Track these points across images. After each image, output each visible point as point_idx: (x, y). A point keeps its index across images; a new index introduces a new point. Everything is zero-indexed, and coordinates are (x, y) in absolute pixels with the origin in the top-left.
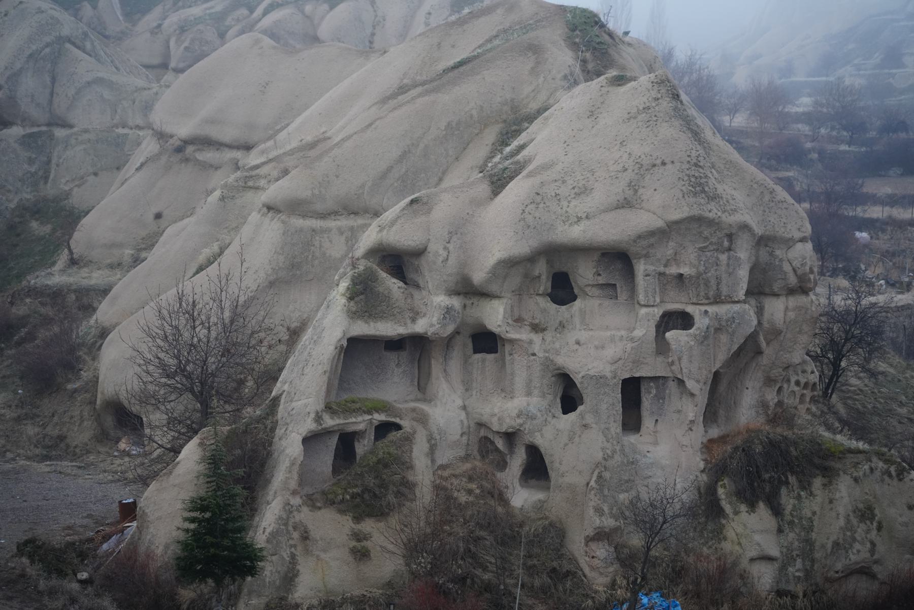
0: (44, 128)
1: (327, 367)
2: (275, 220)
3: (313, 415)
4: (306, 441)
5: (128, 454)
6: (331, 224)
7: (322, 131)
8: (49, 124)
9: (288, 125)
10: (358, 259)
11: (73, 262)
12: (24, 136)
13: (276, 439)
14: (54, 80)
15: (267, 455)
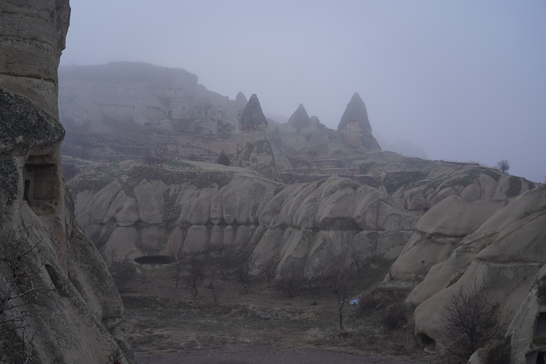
0: (374, 231)
1: (533, 325)
2: (484, 264)
3: (529, 345)
4: (527, 355)
5: (429, 354)
6: (508, 265)
7: (494, 230)
8: (376, 230)
9: (478, 228)
10: (539, 280)
11: (392, 279)
12: (368, 234)
13: (512, 354)
14: (378, 214)
15: (509, 360)
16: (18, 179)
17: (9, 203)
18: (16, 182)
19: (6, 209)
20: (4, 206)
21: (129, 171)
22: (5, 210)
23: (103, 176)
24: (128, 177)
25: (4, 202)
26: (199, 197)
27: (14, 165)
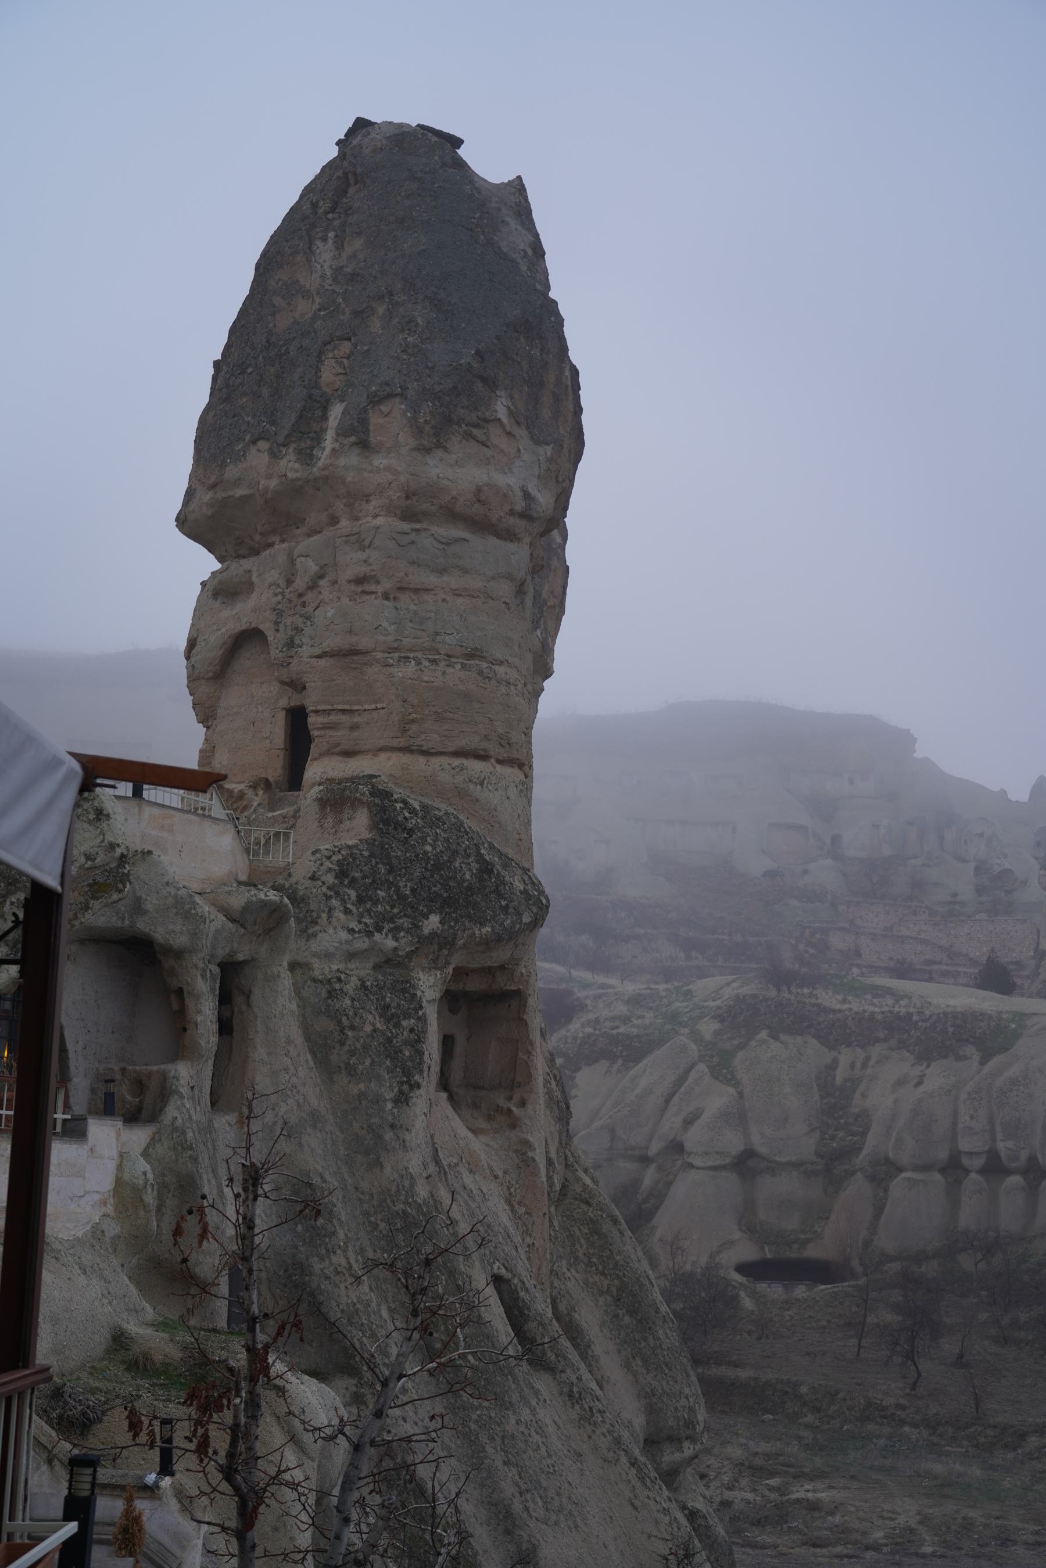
16: (425, 1031)
17: (402, 1100)
18: (419, 1041)
19: (393, 1114)
20: (389, 1105)
21: (719, 1008)
22: (390, 1118)
23: (647, 1022)
24: (716, 1026)
25: (389, 1095)
26: (921, 1088)
27: (416, 994)
